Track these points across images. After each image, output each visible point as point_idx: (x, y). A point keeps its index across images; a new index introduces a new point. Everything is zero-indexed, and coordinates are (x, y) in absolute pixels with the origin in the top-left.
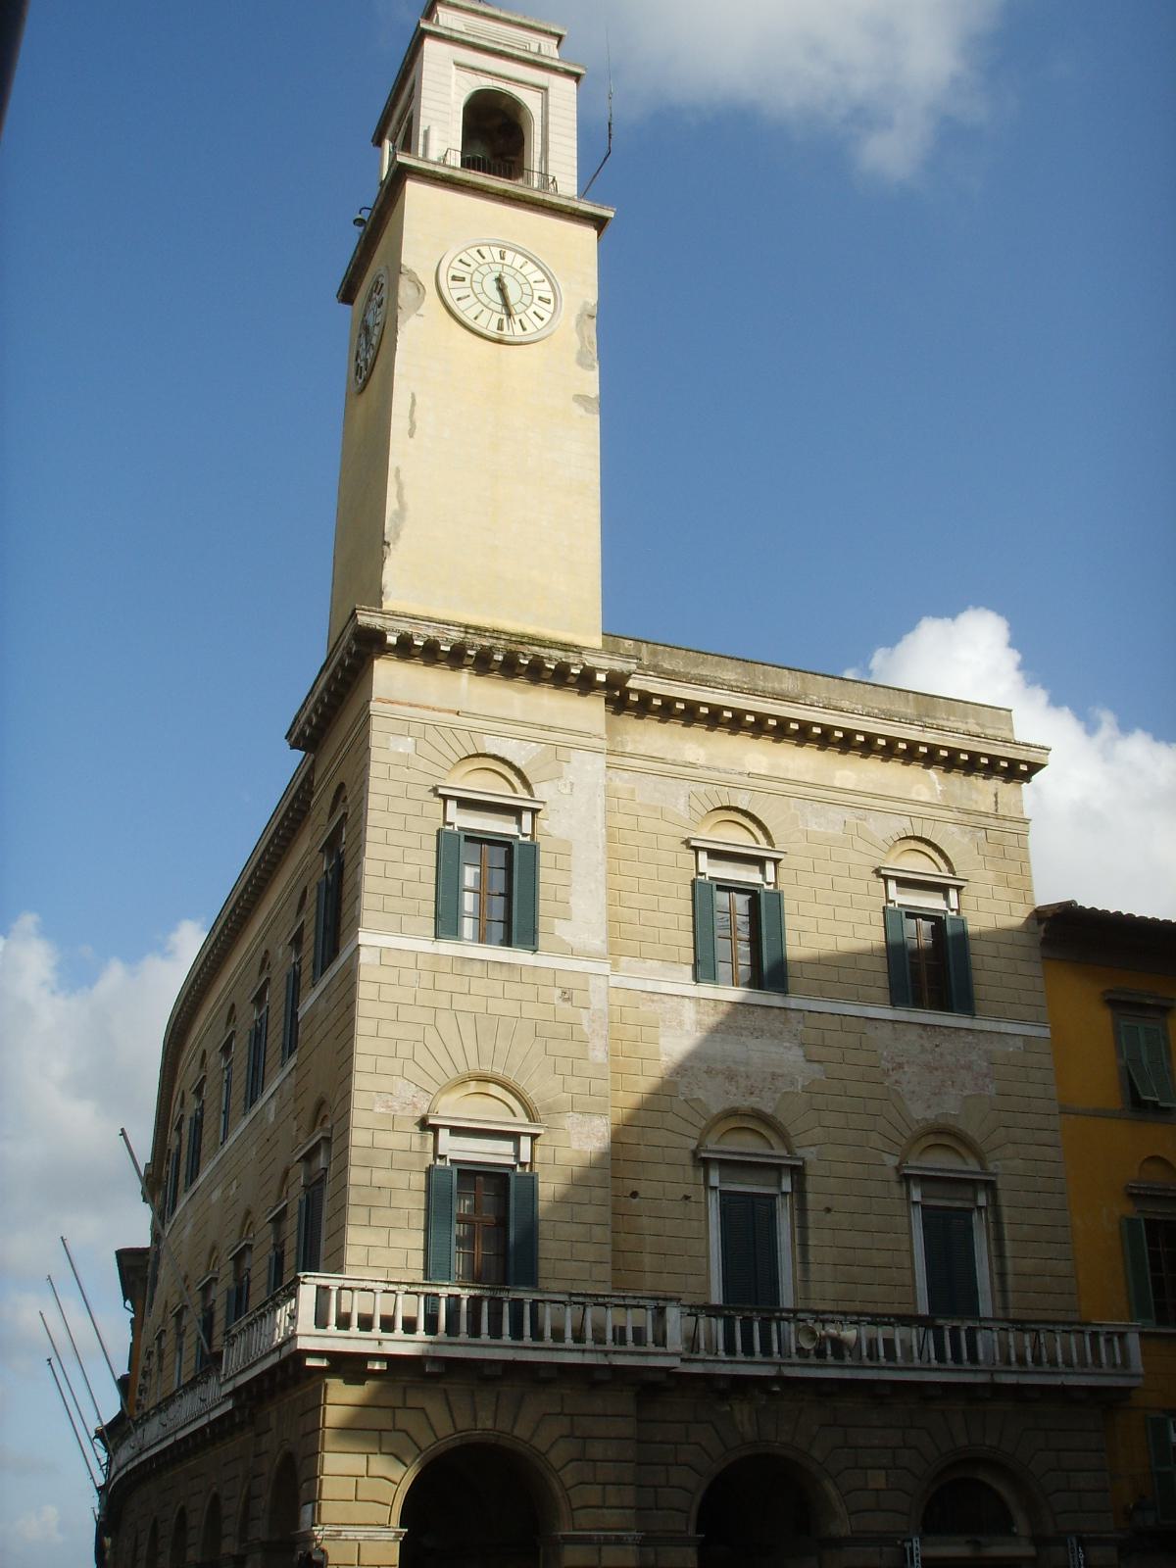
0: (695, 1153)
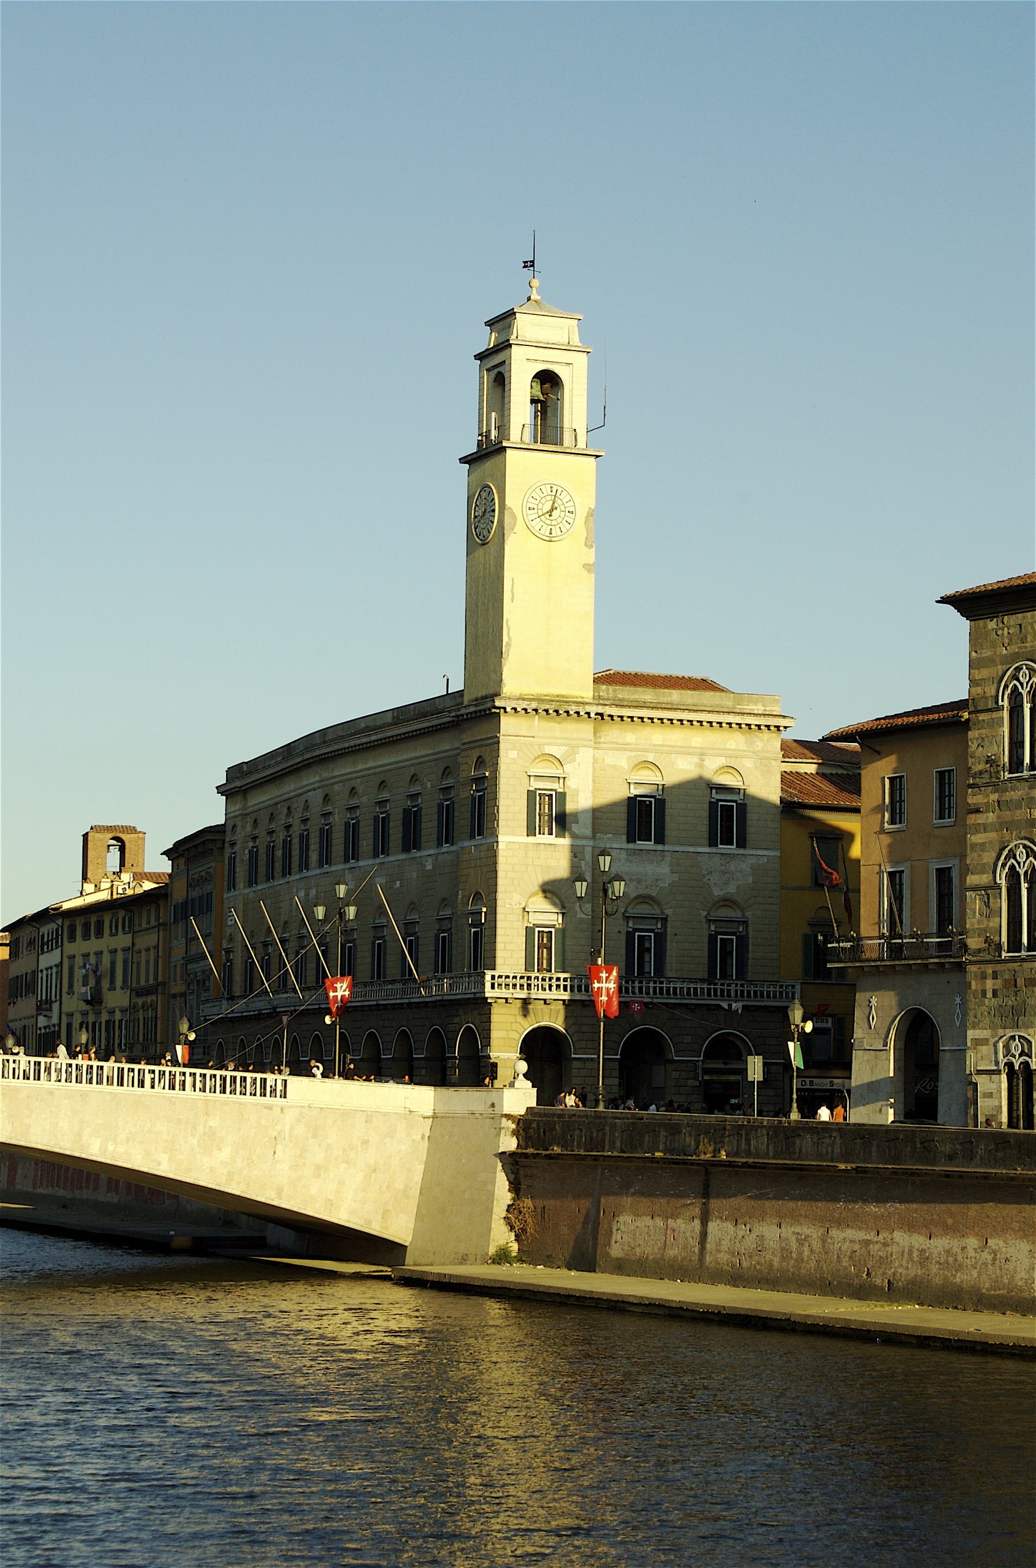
0: (623, 914)
